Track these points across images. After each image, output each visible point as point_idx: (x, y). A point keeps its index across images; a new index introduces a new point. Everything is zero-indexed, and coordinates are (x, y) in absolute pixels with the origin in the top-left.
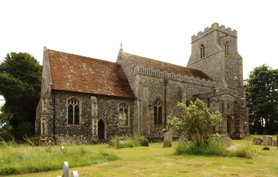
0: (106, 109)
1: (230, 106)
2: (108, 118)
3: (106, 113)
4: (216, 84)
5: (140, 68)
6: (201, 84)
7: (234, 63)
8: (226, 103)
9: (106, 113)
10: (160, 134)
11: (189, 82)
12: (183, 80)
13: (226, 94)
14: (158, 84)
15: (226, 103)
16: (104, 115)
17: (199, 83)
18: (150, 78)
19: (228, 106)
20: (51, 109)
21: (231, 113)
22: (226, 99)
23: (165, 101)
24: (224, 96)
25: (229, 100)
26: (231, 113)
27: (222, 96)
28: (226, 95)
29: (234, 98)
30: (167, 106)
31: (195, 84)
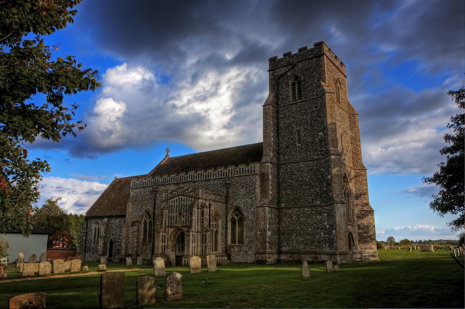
0: (115, 228)
1: (183, 214)
2: (115, 237)
3: (114, 233)
4: (234, 171)
5: (133, 182)
6: (205, 179)
7: (316, 107)
8: (176, 210)
9: (114, 233)
10: (147, 254)
11: (186, 181)
12: (178, 181)
13: (177, 196)
14: (148, 195)
15: (176, 210)
16: (113, 234)
17: (201, 178)
18: (142, 190)
19: (180, 214)
20: (84, 232)
21: (186, 223)
22: (177, 203)
23: (154, 213)
24: (173, 200)
25: (181, 205)
26: (186, 223)
27: (171, 201)
28: (178, 198)
29: (190, 199)
30: (156, 219)
31: (195, 182)
